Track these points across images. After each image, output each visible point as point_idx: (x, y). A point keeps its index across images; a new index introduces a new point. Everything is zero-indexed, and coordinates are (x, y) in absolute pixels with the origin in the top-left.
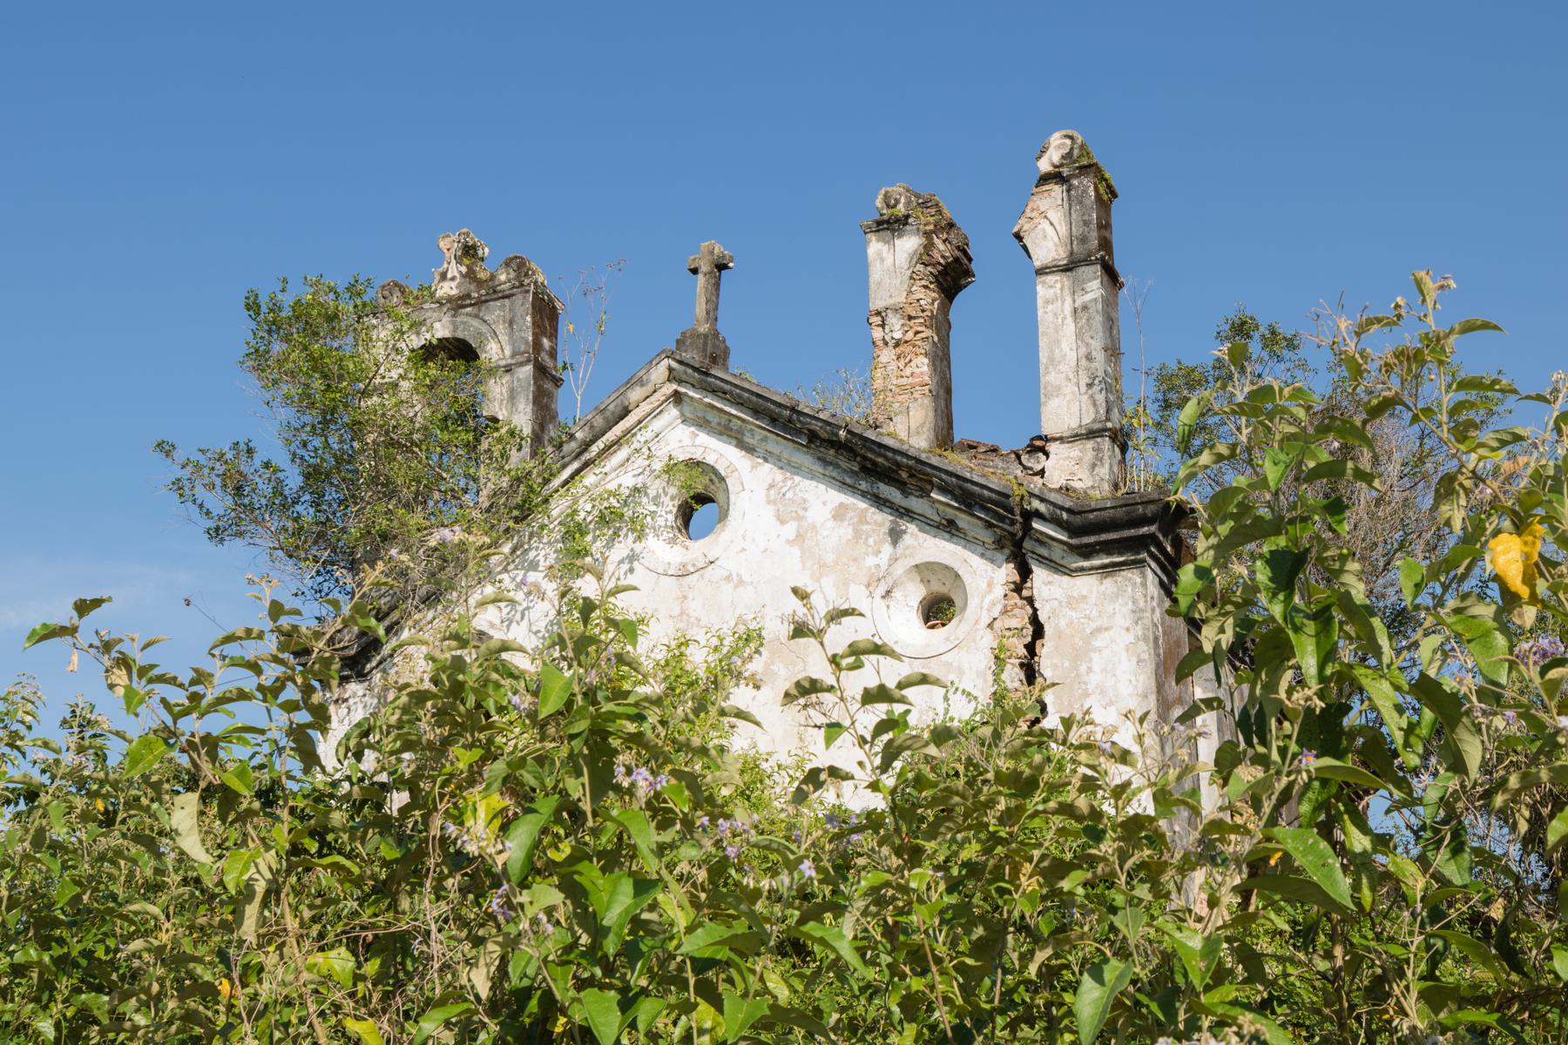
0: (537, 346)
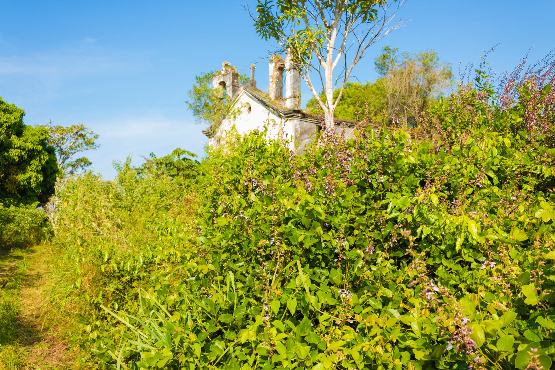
0: (233, 82)
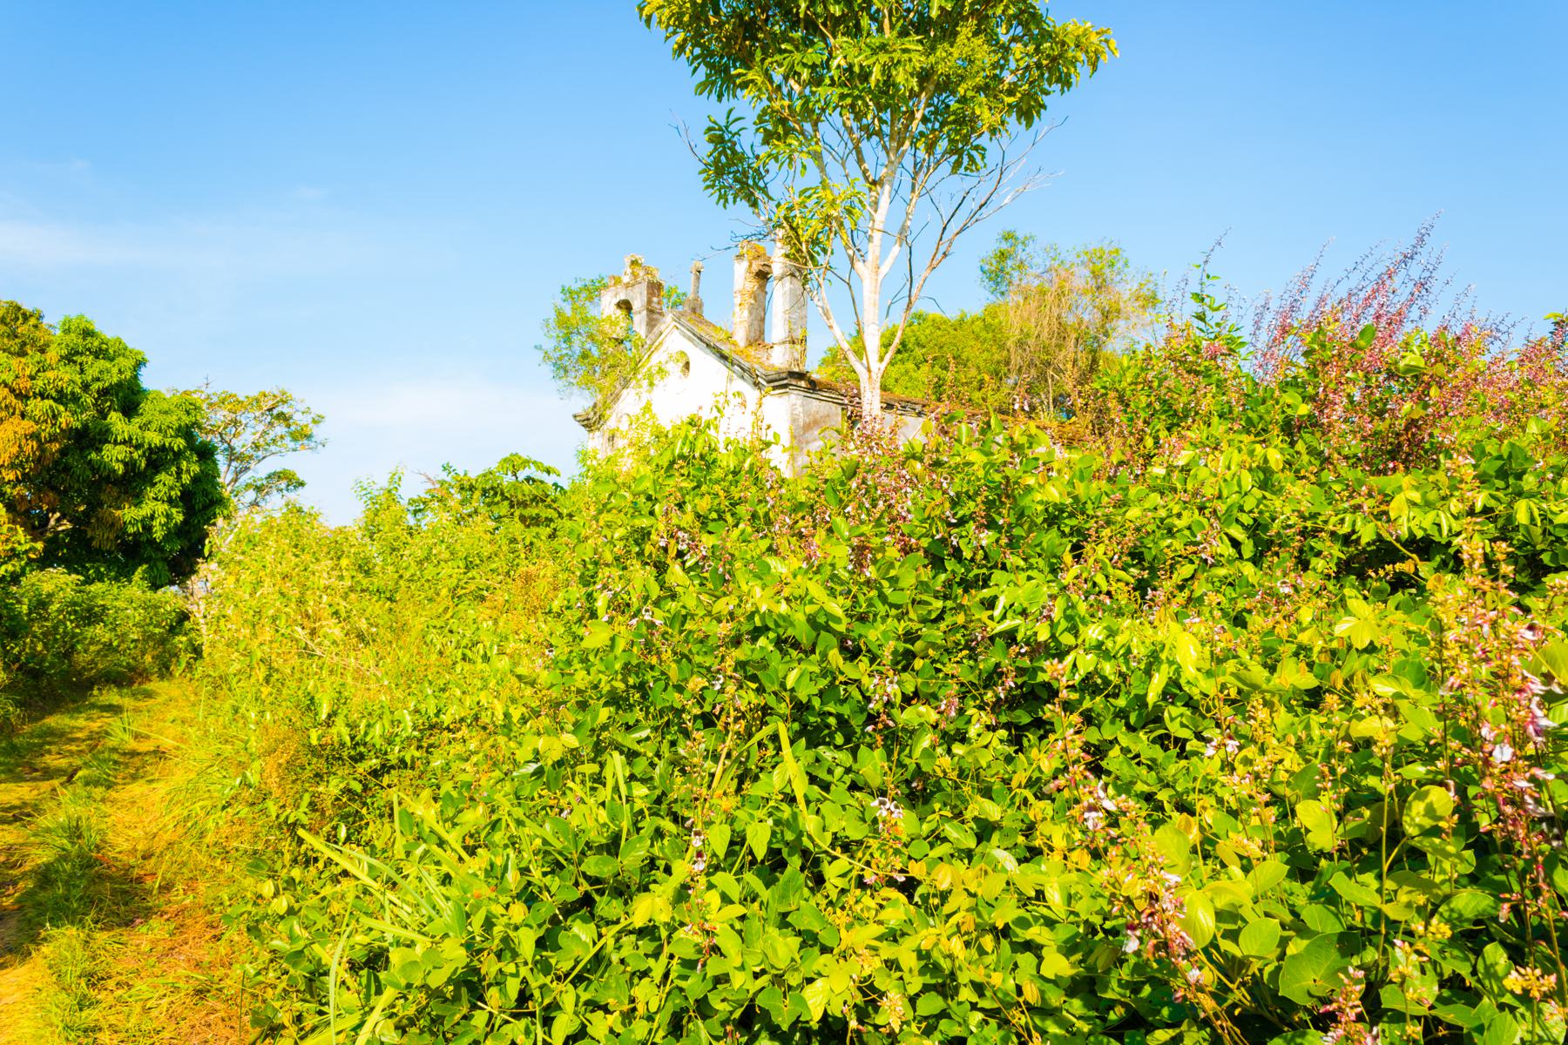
0: (649, 302)
